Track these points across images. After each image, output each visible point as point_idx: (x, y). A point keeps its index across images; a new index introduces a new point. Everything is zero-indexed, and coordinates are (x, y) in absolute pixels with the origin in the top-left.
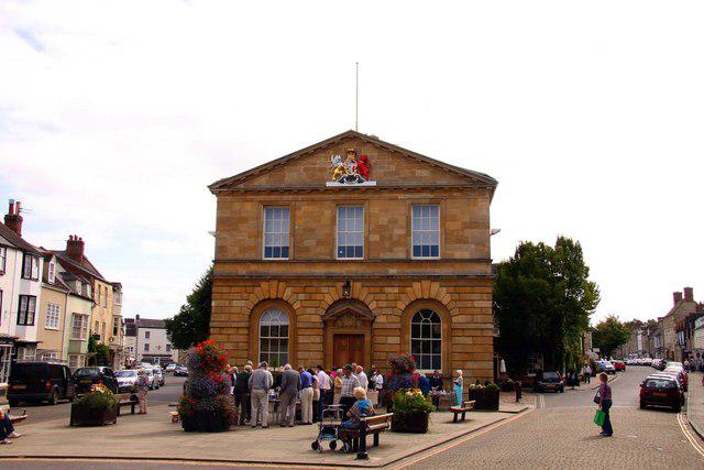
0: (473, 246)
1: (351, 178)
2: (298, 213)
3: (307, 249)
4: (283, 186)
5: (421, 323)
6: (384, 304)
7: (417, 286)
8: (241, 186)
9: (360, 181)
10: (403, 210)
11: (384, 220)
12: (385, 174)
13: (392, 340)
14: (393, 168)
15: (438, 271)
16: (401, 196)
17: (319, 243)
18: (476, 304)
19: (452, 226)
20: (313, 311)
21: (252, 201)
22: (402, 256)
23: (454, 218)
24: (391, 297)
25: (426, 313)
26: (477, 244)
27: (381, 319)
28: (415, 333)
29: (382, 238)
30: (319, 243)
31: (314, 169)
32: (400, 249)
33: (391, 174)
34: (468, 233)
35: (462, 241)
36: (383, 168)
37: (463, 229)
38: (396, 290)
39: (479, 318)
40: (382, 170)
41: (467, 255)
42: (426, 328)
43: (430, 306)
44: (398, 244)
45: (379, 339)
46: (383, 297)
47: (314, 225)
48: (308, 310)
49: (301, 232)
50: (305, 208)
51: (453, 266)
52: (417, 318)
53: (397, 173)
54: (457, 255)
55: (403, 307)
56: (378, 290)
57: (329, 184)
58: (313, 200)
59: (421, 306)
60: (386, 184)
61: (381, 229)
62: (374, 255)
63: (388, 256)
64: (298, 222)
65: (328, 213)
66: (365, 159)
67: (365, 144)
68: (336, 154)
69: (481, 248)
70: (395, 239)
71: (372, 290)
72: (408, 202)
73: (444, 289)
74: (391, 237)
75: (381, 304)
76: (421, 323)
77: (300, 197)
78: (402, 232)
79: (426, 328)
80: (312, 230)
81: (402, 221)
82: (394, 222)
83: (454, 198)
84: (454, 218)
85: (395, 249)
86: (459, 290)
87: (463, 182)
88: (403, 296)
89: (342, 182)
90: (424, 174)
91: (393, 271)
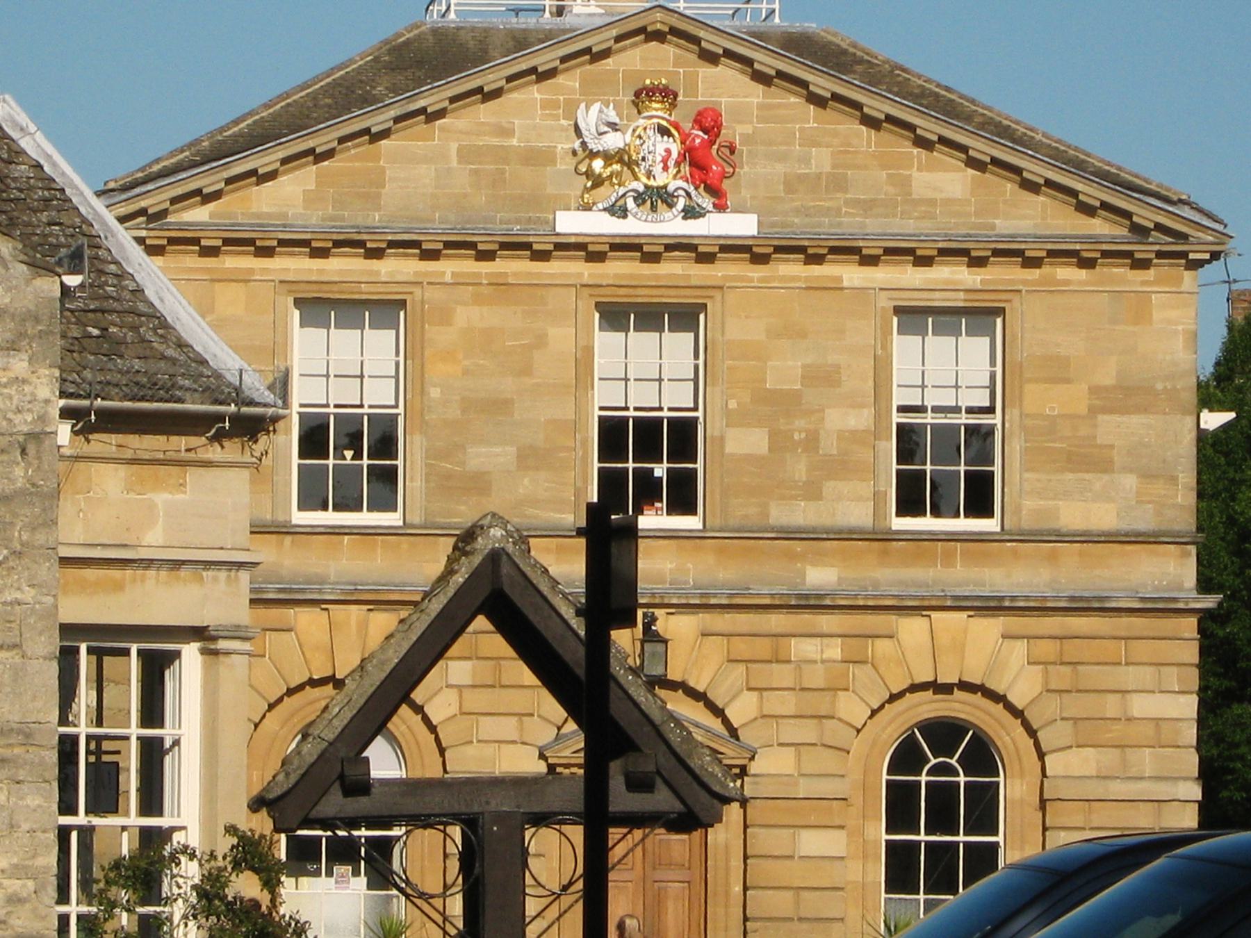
0: (1130, 482)
1: (657, 198)
2: (439, 336)
3: (479, 483)
4: (376, 218)
5: (924, 779)
6: (785, 703)
7: (912, 629)
8: (199, 214)
9: (691, 213)
10: (862, 332)
11: (784, 370)
12: (791, 184)
13: (813, 843)
14: (821, 160)
15: (999, 578)
16: (851, 274)
17: (529, 458)
18: (1142, 706)
19: (1042, 399)
20: (507, 728)
21: (244, 279)
22: (858, 515)
23: (1058, 371)
24: (816, 677)
25: (944, 733)
26: (1147, 476)
27: (771, 764)
28: (900, 808)
29: (779, 442)
30: (529, 458)
31: (502, 155)
32: (845, 487)
33: (812, 183)
34: (1116, 430)
35: (1089, 460)
36: (783, 158)
37: (1093, 411)
38: (834, 650)
39: (1146, 761)
40: (780, 168)
41: (1105, 517)
42: (942, 798)
43: (960, 707)
44: (840, 467)
45: (763, 840)
46: (781, 675)
47: (507, 386)
48: (489, 728)
49: (454, 413)
50: (468, 316)
51: (1053, 558)
52: (906, 757)
53: (838, 183)
54: (1072, 516)
55: (859, 714)
56: (762, 648)
57: (570, 223)
58: (500, 284)
59: (929, 707)
60: (799, 227)
61: (774, 406)
62: (743, 511)
63: (800, 514)
64: (438, 371)
65: (561, 337)
66: (709, 122)
67: (711, 58)
68: (591, 92)
69: (1159, 488)
70: (829, 445)
71: (742, 647)
72: (886, 302)
73: (1021, 647)
74: (812, 441)
75: (785, 703)
76: (924, 779)
77: (448, 268)
78: (861, 419)
79: (942, 798)
80: (498, 406)
81: (859, 380)
82: (823, 377)
83: (1055, 289)
84: (1058, 371)
85: (829, 487)
86: (1073, 650)
87: (1100, 226)
88: (861, 673)
89: (618, 210)
90: (944, 189)
91: (820, 576)
